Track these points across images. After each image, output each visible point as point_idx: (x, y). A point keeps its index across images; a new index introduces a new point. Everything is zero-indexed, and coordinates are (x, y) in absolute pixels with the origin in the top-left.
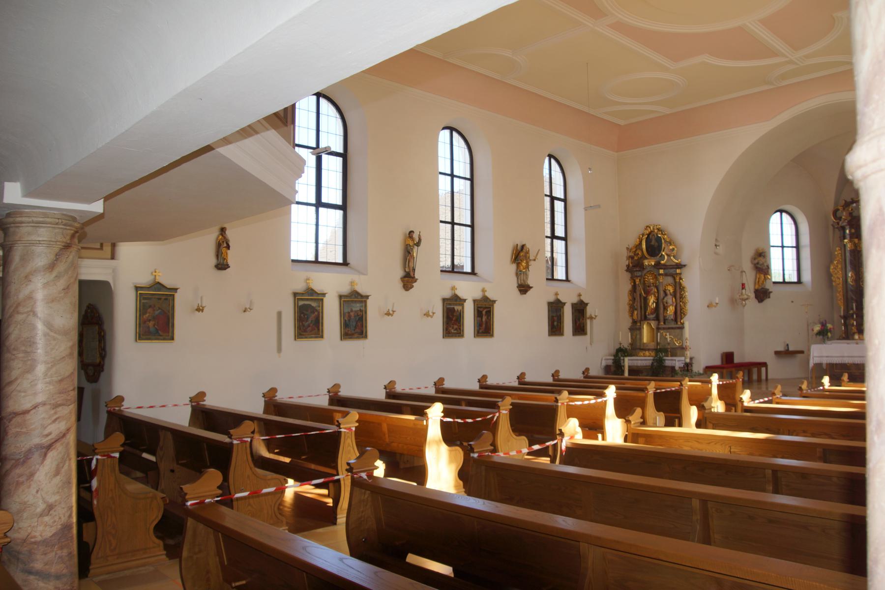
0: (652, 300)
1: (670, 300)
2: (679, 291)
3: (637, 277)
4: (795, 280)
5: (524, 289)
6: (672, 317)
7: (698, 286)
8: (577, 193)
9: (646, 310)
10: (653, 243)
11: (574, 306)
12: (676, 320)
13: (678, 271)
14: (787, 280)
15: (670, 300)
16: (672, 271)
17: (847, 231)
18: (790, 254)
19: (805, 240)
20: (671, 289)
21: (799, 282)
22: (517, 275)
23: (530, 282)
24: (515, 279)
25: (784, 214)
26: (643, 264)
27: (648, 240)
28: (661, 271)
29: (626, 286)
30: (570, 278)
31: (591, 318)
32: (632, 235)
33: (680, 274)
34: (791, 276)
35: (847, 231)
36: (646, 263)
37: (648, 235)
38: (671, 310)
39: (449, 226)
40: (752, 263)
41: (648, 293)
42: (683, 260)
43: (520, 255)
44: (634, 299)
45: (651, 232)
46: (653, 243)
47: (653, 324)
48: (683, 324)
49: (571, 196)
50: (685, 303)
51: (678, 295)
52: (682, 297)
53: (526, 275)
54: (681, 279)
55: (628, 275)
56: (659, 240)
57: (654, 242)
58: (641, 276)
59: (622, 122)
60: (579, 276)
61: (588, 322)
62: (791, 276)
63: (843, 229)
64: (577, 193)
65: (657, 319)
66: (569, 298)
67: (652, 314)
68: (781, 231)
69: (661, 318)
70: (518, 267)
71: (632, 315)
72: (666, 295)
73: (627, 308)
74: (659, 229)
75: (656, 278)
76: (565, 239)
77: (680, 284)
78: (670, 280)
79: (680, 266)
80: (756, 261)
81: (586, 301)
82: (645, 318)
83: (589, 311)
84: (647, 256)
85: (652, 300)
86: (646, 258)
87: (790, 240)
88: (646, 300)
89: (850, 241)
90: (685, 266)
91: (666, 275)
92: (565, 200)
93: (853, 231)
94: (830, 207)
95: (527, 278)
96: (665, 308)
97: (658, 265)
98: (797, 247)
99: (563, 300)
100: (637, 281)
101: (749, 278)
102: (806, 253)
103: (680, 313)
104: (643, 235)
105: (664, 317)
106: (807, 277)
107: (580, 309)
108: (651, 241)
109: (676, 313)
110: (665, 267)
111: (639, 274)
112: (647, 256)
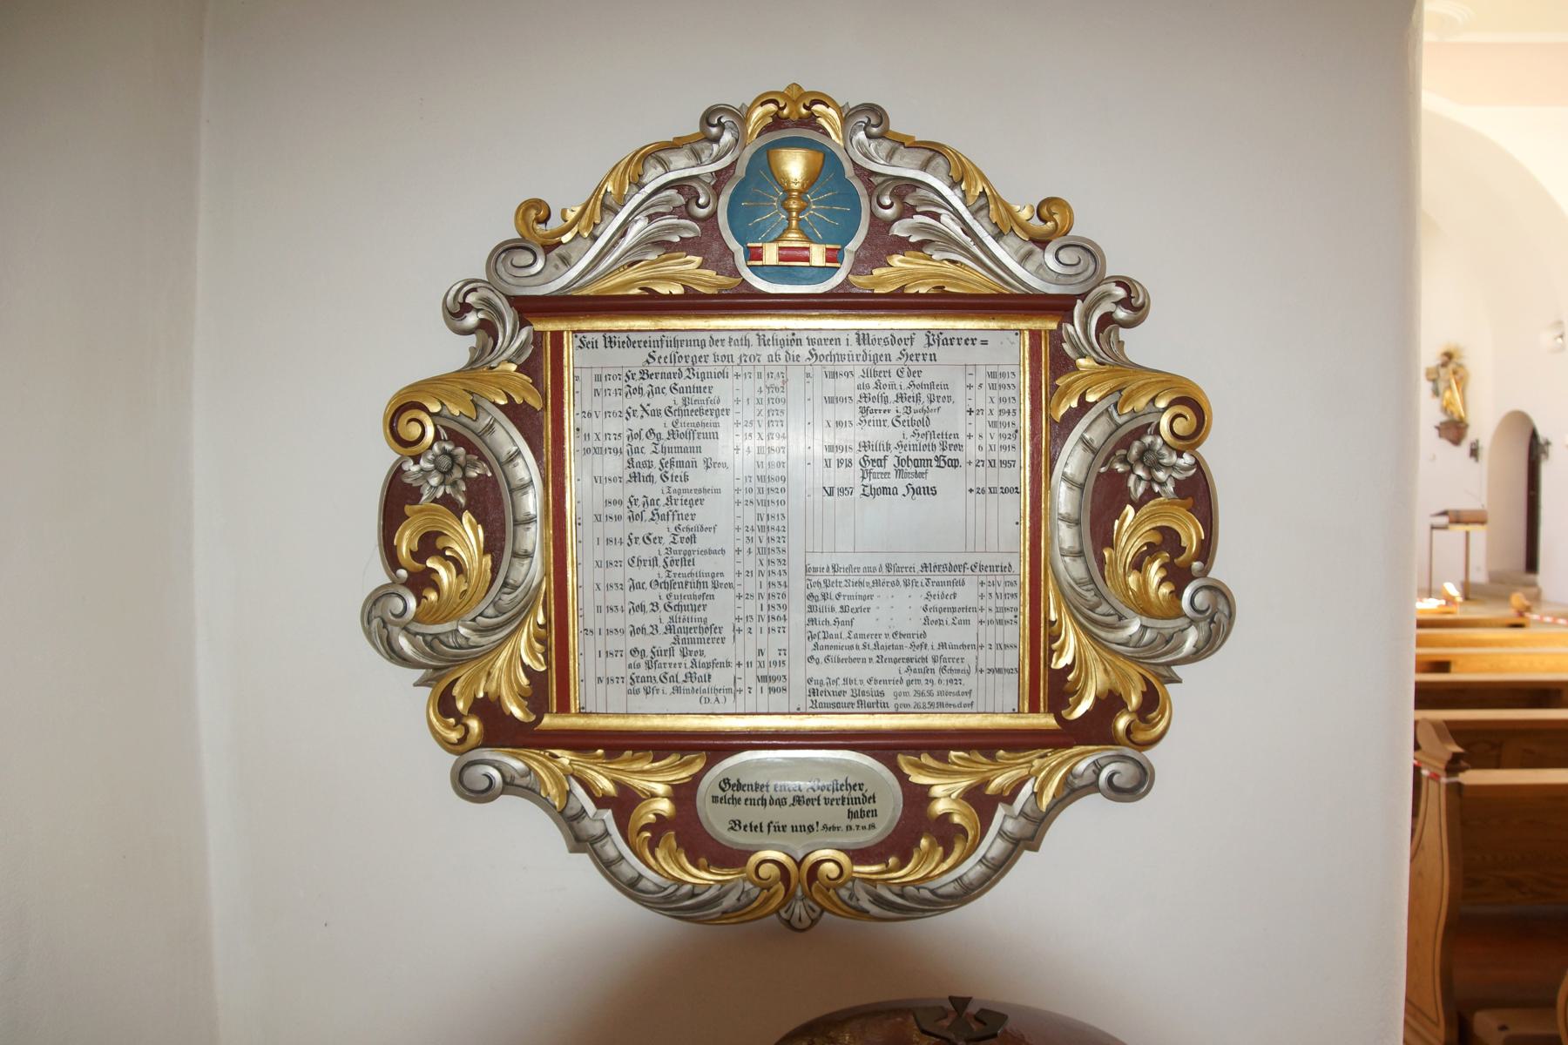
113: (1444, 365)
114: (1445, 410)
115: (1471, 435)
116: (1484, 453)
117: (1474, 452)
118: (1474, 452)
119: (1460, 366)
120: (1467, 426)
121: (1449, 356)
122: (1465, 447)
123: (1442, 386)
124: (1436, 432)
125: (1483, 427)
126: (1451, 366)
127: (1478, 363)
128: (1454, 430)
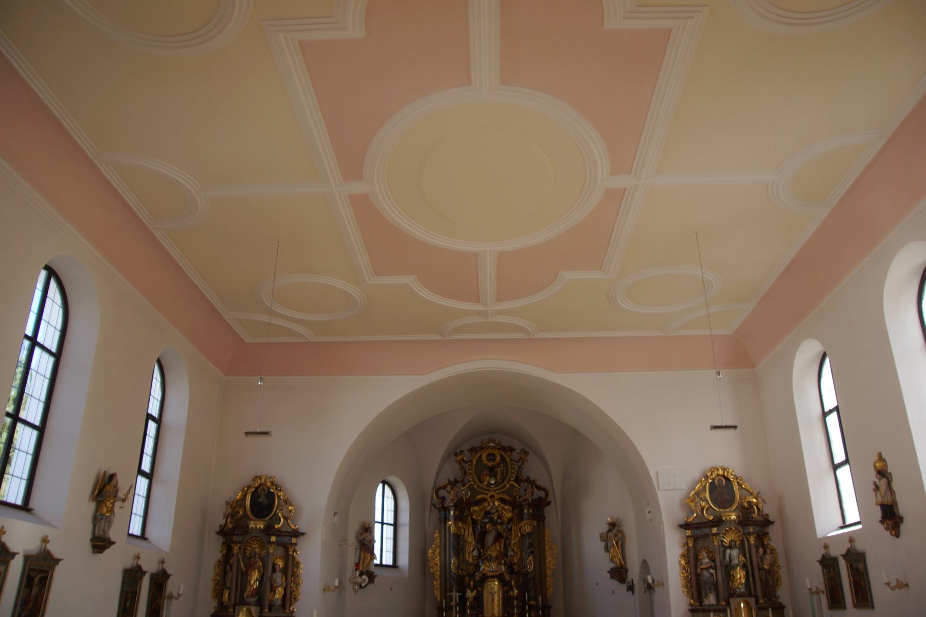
0: (255, 575)
1: (279, 578)
2: (291, 568)
3: (235, 542)
4: (390, 562)
5: (100, 543)
6: (280, 602)
7: (314, 559)
8: (177, 415)
9: (243, 590)
10: (261, 499)
11: (153, 576)
12: (283, 606)
13: (294, 540)
14: (384, 563)
15: (279, 578)
16: (286, 539)
17: (452, 513)
18: (389, 531)
19: (405, 518)
20: (280, 564)
21: (395, 565)
22: (96, 519)
23: (113, 534)
24: (91, 526)
25: (386, 487)
26: (247, 526)
27: (255, 495)
28: (273, 539)
29: (214, 551)
30: (148, 535)
31: (171, 597)
32: (231, 484)
33: (296, 544)
34: (388, 560)
35: (452, 513)
36: (252, 525)
37: (257, 488)
38: (280, 591)
39: (8, 420)
40: (357, 537)
41: (250, 566)
42: (301, 526)
43: (106, 491)
44: (224, 574)
45: (262, 484)
46: (261, 499)
47: (255, 610)
48: (293, 612)
49: (166, 418)
50: (297, 584)
51: (290, 573)
52: (295, 575)
53: (109, 521)
54: (295, 551)
55: (220, 539)
56: (271, 497)
57: (264, 500)
58: (242, 542)
59: (248, 339)
60: (162, 534)
61: (166, 601)
62: (388, 560)
63: (445, 510)
64: (177, 415)
65: (260, 604)
66: (150, 566)
67: (252, 596)
68: (384, 505)
69: (267, 604)
70: (98, 507)
71: (218, 595)
72: (274, 570)
73: (211, 585)
74: (272, 483)
75: (263, 547)
76: (149, 476)
77: (294, 557)
78: (280, 551)
79: (297, 534)
80: (362, 537)
81: (169, 572)
82: (242, 602)
83: (171, 586)
84: (250, 515)
85: (255, 575)
86: (251, 519)
87: (389, 518)
88: (245, 576)
89: (455, 524)
90: (303, 534)
91: (278, 544)
92: (159, 421)
93: (457, 513)
94: (429, 484)
95: (109, 527)
96: (273, 590)
97: (269, 530)
98: (395, 525)
99: (145, 568)
100: (236, 549)
101: (352, 556)
102: (404, 533)
103: (289, 598)
104: (249, 487)
105: (272, 601)
106: (404, 561)
107: (160, 580)
108: (259, 496)
109: (284, 596)
110: (279, 533)
111: (240, 539)
112: (250, 515)
113: (608, 532)
114: (612, 560)
115: (629, 579)
116: (636, 588)
117: (631, 588)
118: (631, 588)
119: (621, 532)
120: (627, 570)
121: (613, 525)
122: (625, 587)
123: (609, 545)
124: (608, 575)
125: (634, 573)
126: (614, 531)
127: (630, 529)
128: (619, 573)
